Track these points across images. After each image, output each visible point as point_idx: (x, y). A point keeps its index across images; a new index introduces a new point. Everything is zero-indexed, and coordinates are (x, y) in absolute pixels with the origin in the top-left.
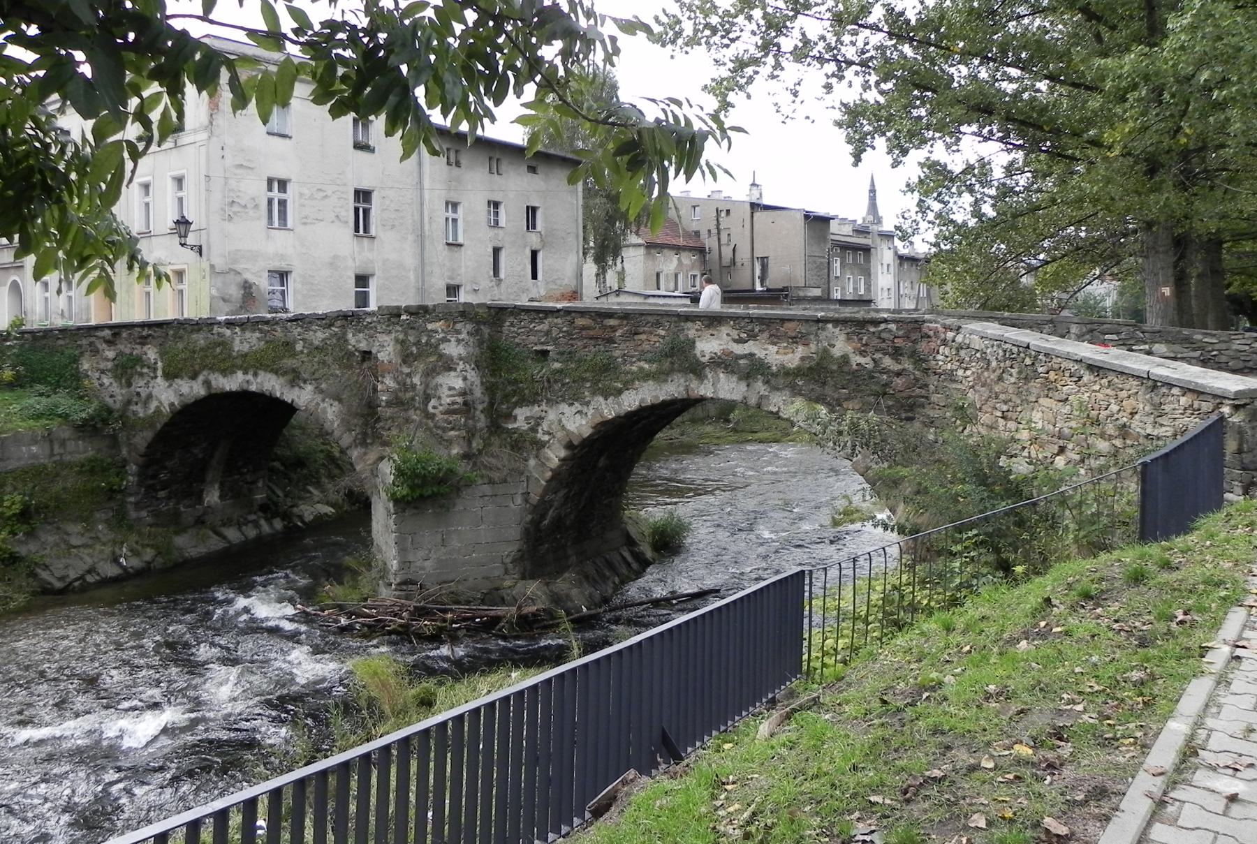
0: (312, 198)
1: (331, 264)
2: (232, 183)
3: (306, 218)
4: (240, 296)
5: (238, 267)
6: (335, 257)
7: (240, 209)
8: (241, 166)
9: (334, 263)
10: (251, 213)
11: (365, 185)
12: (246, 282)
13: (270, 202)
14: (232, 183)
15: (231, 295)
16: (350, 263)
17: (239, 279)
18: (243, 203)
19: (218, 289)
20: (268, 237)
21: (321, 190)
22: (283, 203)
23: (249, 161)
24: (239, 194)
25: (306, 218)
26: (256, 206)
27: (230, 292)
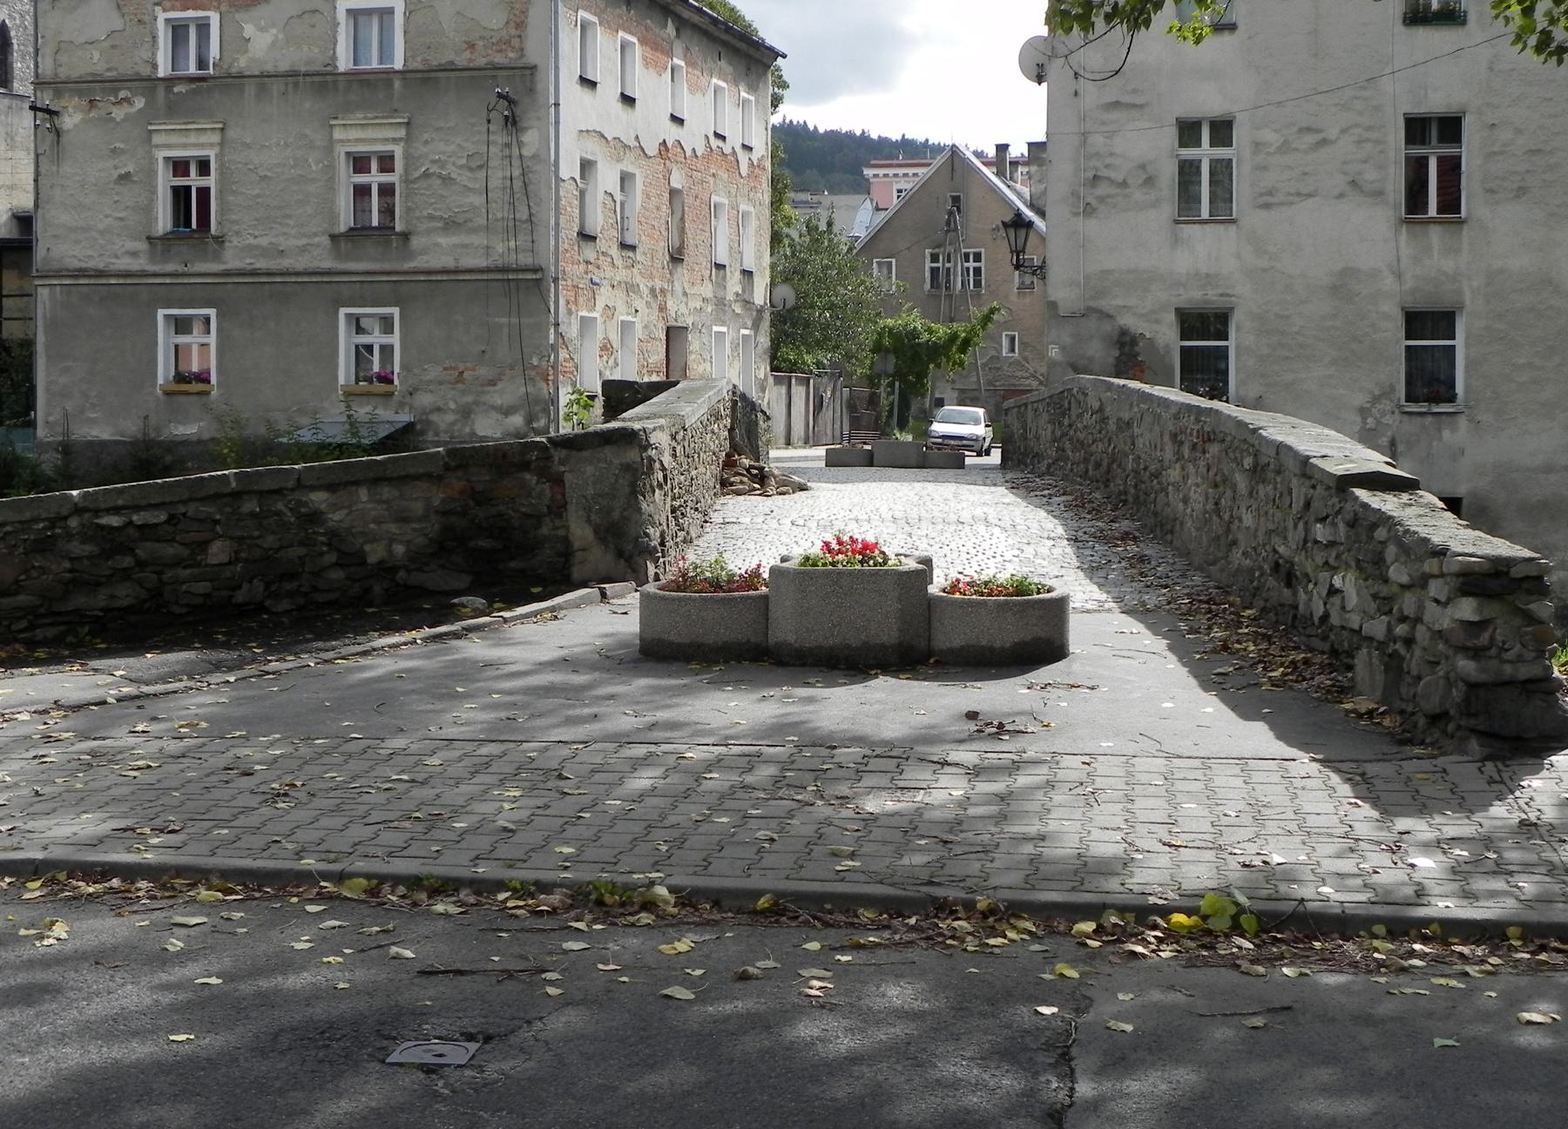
0: (1285, 148)
2: (1097, 140)
3: (1270, 193)
4: (1111, 360)
5: (1105, 304)
6: (1347, 273)
7: (1112, 190)
8: (1116, 105)
9: (1343, 285)
10: (1138, 195)
11: (1436, 103)
12: (1124, 332)
13: (1188, 171)
14: (1097, 140)
15: (1091, 359)
16: (1389, 283)
17: (1107, 327)
18: (1119, 177)
19: (1063, 348)
20: (1176, 241)
21: (1309, 130)
22: (1222, 171)
23: (1134, 91)
24: (1108, 161)
25: (1270, 193)
26: (1150, 181)
27: (1090, 353)
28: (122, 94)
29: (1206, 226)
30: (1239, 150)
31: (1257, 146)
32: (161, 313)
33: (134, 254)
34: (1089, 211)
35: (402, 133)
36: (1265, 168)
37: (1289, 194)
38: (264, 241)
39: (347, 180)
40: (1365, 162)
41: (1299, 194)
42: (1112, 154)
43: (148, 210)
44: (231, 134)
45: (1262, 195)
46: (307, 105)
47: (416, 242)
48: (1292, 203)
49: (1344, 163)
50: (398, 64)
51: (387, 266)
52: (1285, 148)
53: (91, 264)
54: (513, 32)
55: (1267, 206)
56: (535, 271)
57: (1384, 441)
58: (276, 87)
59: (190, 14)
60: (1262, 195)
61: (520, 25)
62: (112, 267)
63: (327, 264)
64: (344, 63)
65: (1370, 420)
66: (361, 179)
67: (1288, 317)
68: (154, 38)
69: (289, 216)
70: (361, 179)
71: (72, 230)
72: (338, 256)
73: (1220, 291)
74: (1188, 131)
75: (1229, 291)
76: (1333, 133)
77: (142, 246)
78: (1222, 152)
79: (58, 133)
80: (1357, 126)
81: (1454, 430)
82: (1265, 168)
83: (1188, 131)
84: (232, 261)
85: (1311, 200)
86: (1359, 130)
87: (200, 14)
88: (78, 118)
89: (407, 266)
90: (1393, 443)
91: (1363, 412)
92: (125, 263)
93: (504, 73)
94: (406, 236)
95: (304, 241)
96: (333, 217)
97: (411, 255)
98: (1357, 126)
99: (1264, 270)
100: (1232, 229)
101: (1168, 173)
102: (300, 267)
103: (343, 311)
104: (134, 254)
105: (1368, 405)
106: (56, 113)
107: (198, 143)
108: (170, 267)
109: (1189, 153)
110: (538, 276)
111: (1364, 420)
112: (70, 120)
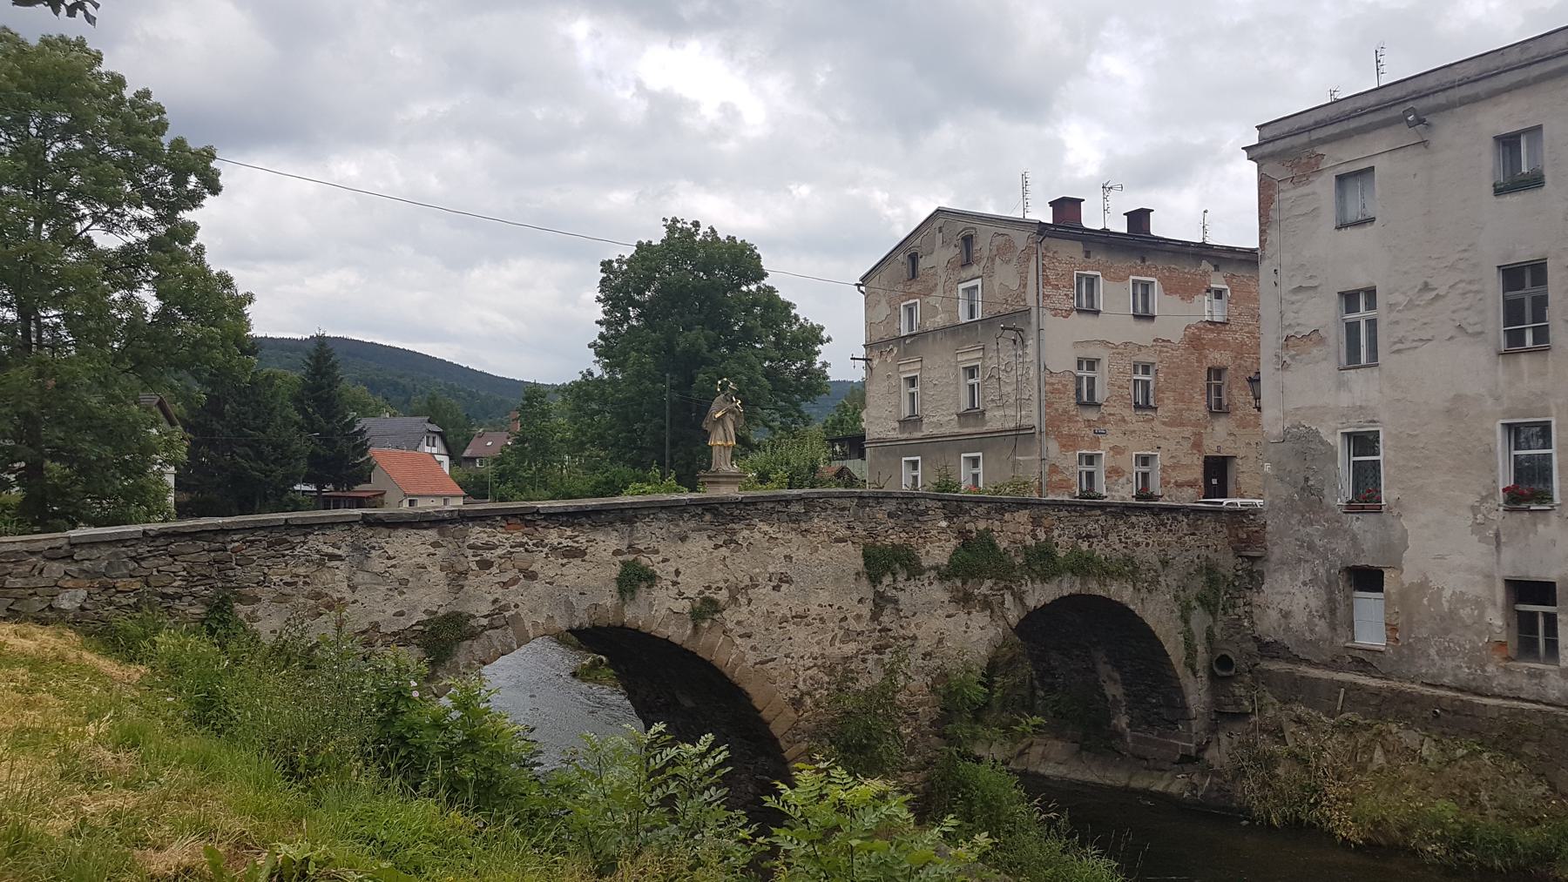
1: (1448, 411)
2: (1290, 317)
3: (1401, 342)
8: (1300, 289)
9: (1455, 409)
14: (1290, 317)
20: (1342, 385)
28: (891, 346)
29: (1358, 371)
30: (1380, 313)
31: (1391, 307)
32: (904, 459)
33: (895, 429)
34: (1284, 366)
35: (980, 354)
36: (1397, 323)
37: (1414, 341)
38: (935, 419)
39: (964, 382)
40: (1467, 309)
41: (1421, 340)
42: (1298, 325)
43: (898, 406)
44: (924, 362)
45: (1395, 343)
46: (949, 343)
47: (988, 415)
48: (1416, 348)
49: (1454, 312)
50: (980, 318)
51: (978, 430)
52: (1411, 305)
53: (882, 436)
54: (1023, 290)
55: (1399, 351)
56: (1031, 429)
57: (1491, 533)
58: (939, 336)
59: (911, 302)
60: (1395, 343)
61: (1025, 286)
62: (889, 437)
63: (957, 430)
64: (964, 318)
65: (1479, 516)
66: (971, 381)
67: (1416, 436)
68: (900, 316)
69: (943, 405)
70: (971, 381)
71: (876, 418)
72: (961, 425)
73: (1369, 419)
74: (1350, 299)
75: (1375, 419)
76: (1442, 292)
77: (897, 425)
78: (1371, 314)
79: (871, 369)
80: (1461, 281)
81: (1547, 525)
82: (1397, 323)
83: (1350, 299)
84: (926, 430)
85: (1430, 343)
86: (1462, 285)
87: (913, 301)
88: (877, 360)
89: (984, 429)
90: (1497, 536)
91: (1474, 509)
92: (893, 435)
93: (1017, 314)
94: (983, 413)
95: (949, 418)
96: (959, 408)
97: (984, 423)
98: (1461, 281)
99: (1398, 400)
100: (1376, 369)
101: (1336, 338)
102: (948, 433)
103: (963, 455)
104: (895, 429)
105: (1477, 504)
106: (870, 360)
107: (912, 370)
108: (905, 436)
109: (1352, 317)
110: (1032, 431)
111: (1475, 515)
112: (875, 362)
